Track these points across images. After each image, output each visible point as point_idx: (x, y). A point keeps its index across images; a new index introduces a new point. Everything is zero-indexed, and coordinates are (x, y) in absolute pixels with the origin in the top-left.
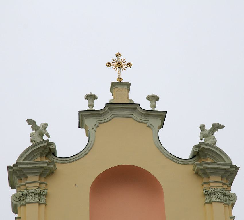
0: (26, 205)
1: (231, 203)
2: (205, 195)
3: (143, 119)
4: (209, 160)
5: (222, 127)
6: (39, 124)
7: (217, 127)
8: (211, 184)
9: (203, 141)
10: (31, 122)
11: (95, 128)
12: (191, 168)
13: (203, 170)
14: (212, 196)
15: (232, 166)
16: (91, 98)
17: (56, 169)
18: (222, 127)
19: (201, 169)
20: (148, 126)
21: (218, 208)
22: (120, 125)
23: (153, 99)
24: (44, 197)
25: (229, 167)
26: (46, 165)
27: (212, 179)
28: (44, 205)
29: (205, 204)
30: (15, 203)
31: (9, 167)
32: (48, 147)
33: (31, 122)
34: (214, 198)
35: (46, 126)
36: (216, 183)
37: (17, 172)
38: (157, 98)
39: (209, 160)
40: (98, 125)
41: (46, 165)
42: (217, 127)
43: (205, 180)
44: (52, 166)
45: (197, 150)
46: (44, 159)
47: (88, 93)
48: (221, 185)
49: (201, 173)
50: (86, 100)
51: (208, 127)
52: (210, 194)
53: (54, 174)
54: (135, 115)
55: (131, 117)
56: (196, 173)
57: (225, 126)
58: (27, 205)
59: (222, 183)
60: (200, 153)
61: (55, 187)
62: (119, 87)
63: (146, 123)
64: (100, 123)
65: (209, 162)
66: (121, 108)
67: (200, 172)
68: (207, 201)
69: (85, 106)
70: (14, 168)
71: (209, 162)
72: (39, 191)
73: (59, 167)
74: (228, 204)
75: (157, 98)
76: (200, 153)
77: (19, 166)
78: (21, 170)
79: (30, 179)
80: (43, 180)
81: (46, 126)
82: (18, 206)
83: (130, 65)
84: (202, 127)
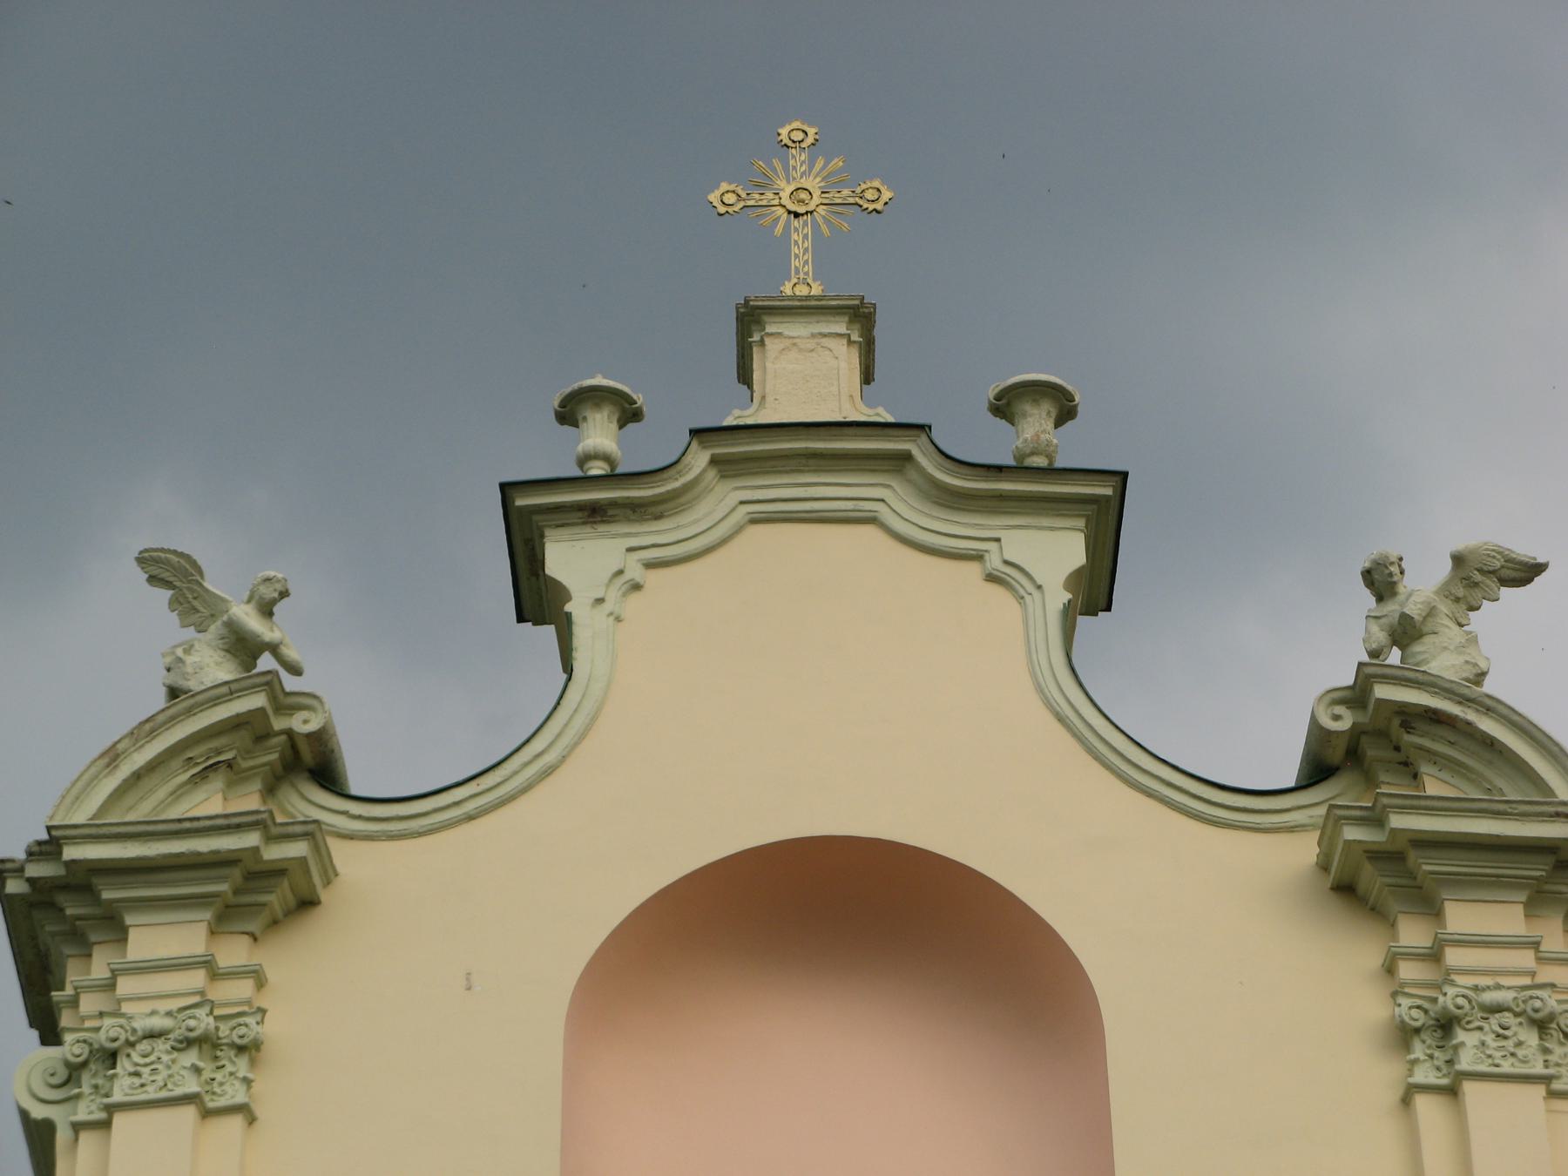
0: (106, 1125)
2: (1405, 1035)
8: (1453, 956)
11: (613, 595)
12: (1303, 851)
13: (1392, 856)
14: (1461, 1036)
17: (330, 873)
18: (1525, 573)
19: (1375, 855)
20: (992, 578)
24: (242, 1066)
26: (251, 839)
27: (1461, 917)
28: (237, 1121)
29: (1406, 1101)
30: (38, 1112)
32: (278, 724)
34: (1470, 1047)
37: (61, 899)
40: (635, 572)
41: (251, 839)
43: (1413, 933)
44: (297, 849)
45: (1345, 725)
46: (249, 801)
48: (1526, 959)
49: (1373, 883)
50: (566, 427)
52: (1446, 1025)
53: (318, 910)
55: (872, 520)
56: (1346, 889)
58: (119, 1120)
59: (1535, 945)
63: (978, 557)
64: (650, 565)
65: (1438, 804)
67: (1372, 879)
68: (1425, 1075)
69: (545, 453)
70: (33, 871)
71: (1438, 804)
72: (203, 1022)
73: (358, 866)
76: (1372, 751)
77: (71, 853)
78: (84, 879)
79: (150, 938)
80: (234, 952)
82: (62, 1136)
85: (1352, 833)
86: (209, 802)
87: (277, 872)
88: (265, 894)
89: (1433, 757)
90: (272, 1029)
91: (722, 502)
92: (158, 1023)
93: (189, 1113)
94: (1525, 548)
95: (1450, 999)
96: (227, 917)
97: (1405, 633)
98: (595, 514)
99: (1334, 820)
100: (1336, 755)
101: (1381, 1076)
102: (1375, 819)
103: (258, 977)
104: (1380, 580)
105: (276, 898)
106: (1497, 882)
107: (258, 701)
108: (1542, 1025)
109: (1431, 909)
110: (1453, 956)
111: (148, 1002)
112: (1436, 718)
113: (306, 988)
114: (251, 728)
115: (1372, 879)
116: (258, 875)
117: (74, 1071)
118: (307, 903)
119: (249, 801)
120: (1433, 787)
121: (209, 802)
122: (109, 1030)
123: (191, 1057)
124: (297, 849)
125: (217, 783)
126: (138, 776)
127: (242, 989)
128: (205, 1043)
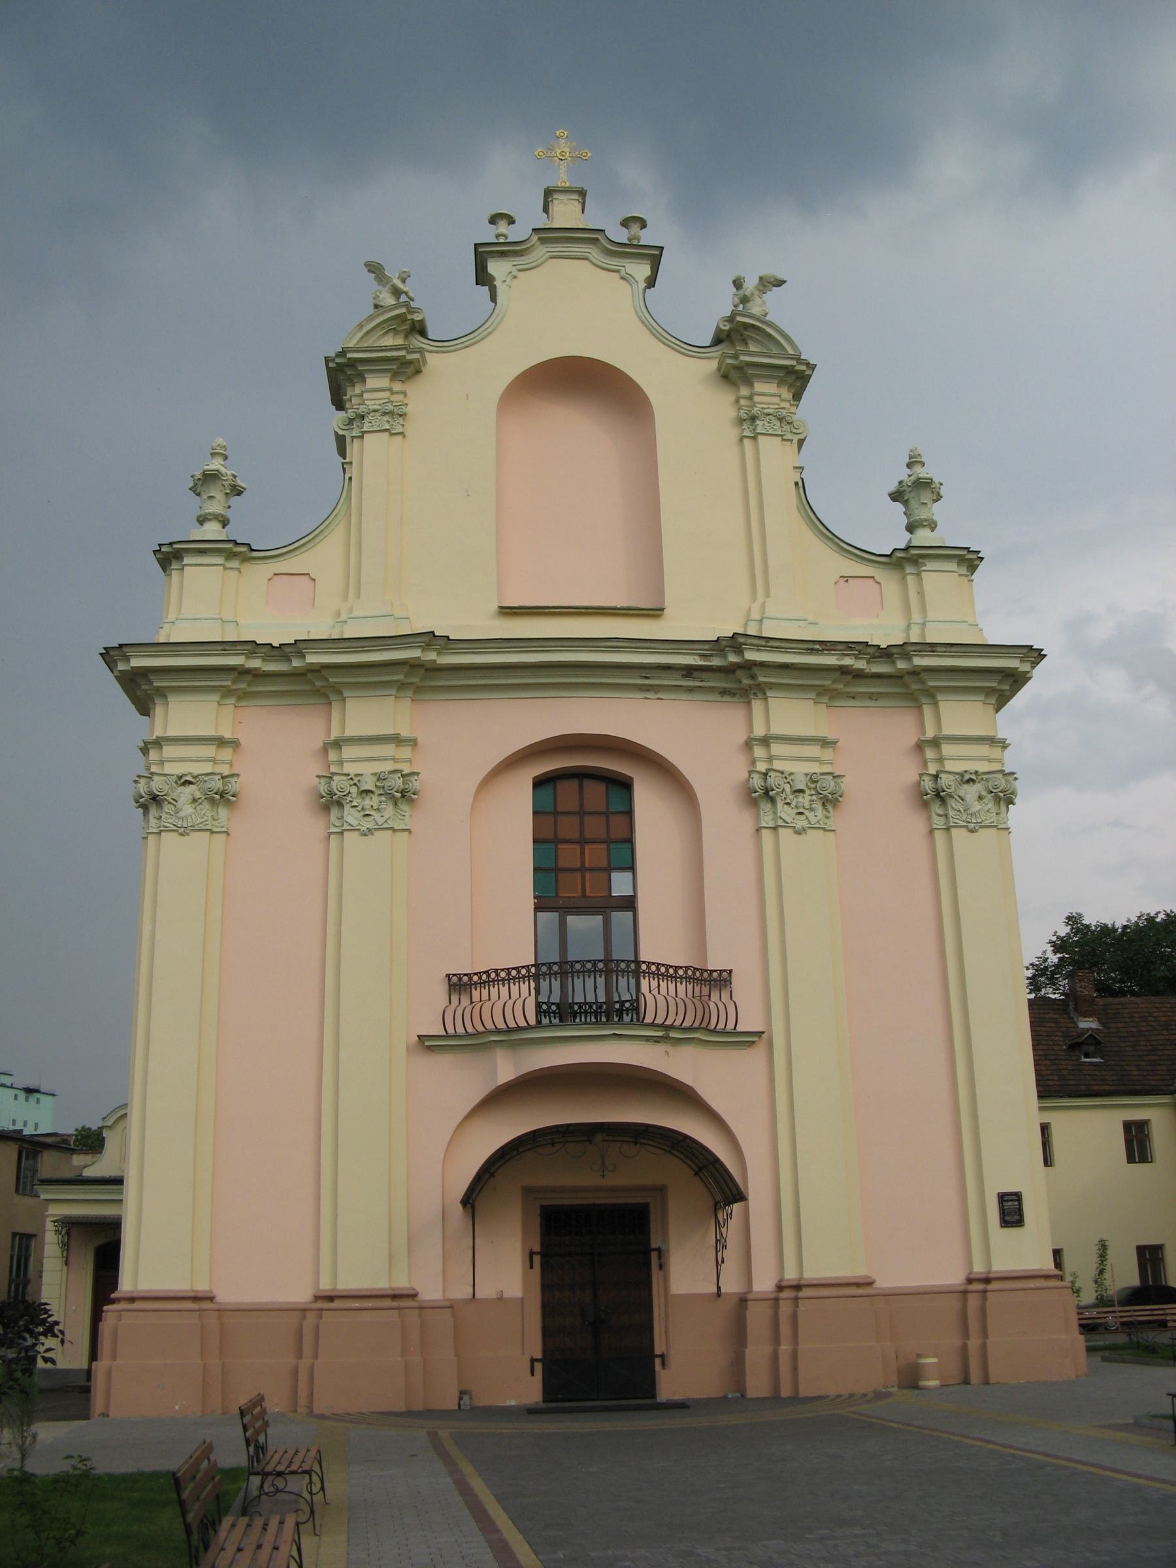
0: (362, 437)
1: (796, 438)
2: (741, 421)
8: (756, 399)
10: (375, 269)
11: (508, 280)
12: (713, 365)
15: (799, 360)
17: (425, 362)
18: (780, 283)
19: (735, 368)
20: (622, 278)
25: (793, 363)
26: (403, 353)
27: (759, 387)
28: (400, 437)
30: (341, 432)
31: (327, 360)
32: (409, 317)
33: (375, 269)
36: (769, 394)
37: (346, 369)
39: (752, 348)
40: (515, 273)
41: (403, 353)
43: (744, 391)
44: (416, 356)
45: (727, 328)
46: (400, 341)
48: (777, 400)
49: (733, 376)
52: (753, 419)
53: (421, 375)
57: (784, 282)
58: (366, 436)
62: (562, 197)
63: (618, 271)
64: (520, 270)
65: (753, 353)
68: (746, 433)
69: (488, 234)
70: (338, 360)
71: (753, 353)
72: (390, 407)
73: (435, 362)
74: (791, 441)
76: (734, 336)
77: (349, 355)
78: (353, 363)
79: (372, 382)
80: (397, 386)
82: (348, 440)
85: (729, 361)
86: (389, 341)
87: (410, 362)
88: (406, 369)
89: (752, 339)
90: (408, 410)
91: (541, 251)
92: (376, 407)
93: (386, 434)
94: (781, 276)
95: (755, 411)
96: (395, 376)
97: (745, 300)
98: (503, 254)
99: (723, 357)
100: (723, 336)
101: (733, 433)
102: (735, 357)
103: (405, 394)
104: (738, 284)
106: (770, 377)
107: (403, 310)
109: (750, 384)
110: (756, 399)
111: (373, 401)
112: (753, 326)
113: (419, 397)
114: (401, 318)
115: (734, 375)
116: (404, 363)
117: (351, 421)
118: (418, 372)
119: (400, 341)
120: (752, 348)
121: (389, 341)
122: (362, 409)
123: (386, 418)
124: (416, 356)
125: (391, 335)
126: (368, 332)
127: (401, 397)
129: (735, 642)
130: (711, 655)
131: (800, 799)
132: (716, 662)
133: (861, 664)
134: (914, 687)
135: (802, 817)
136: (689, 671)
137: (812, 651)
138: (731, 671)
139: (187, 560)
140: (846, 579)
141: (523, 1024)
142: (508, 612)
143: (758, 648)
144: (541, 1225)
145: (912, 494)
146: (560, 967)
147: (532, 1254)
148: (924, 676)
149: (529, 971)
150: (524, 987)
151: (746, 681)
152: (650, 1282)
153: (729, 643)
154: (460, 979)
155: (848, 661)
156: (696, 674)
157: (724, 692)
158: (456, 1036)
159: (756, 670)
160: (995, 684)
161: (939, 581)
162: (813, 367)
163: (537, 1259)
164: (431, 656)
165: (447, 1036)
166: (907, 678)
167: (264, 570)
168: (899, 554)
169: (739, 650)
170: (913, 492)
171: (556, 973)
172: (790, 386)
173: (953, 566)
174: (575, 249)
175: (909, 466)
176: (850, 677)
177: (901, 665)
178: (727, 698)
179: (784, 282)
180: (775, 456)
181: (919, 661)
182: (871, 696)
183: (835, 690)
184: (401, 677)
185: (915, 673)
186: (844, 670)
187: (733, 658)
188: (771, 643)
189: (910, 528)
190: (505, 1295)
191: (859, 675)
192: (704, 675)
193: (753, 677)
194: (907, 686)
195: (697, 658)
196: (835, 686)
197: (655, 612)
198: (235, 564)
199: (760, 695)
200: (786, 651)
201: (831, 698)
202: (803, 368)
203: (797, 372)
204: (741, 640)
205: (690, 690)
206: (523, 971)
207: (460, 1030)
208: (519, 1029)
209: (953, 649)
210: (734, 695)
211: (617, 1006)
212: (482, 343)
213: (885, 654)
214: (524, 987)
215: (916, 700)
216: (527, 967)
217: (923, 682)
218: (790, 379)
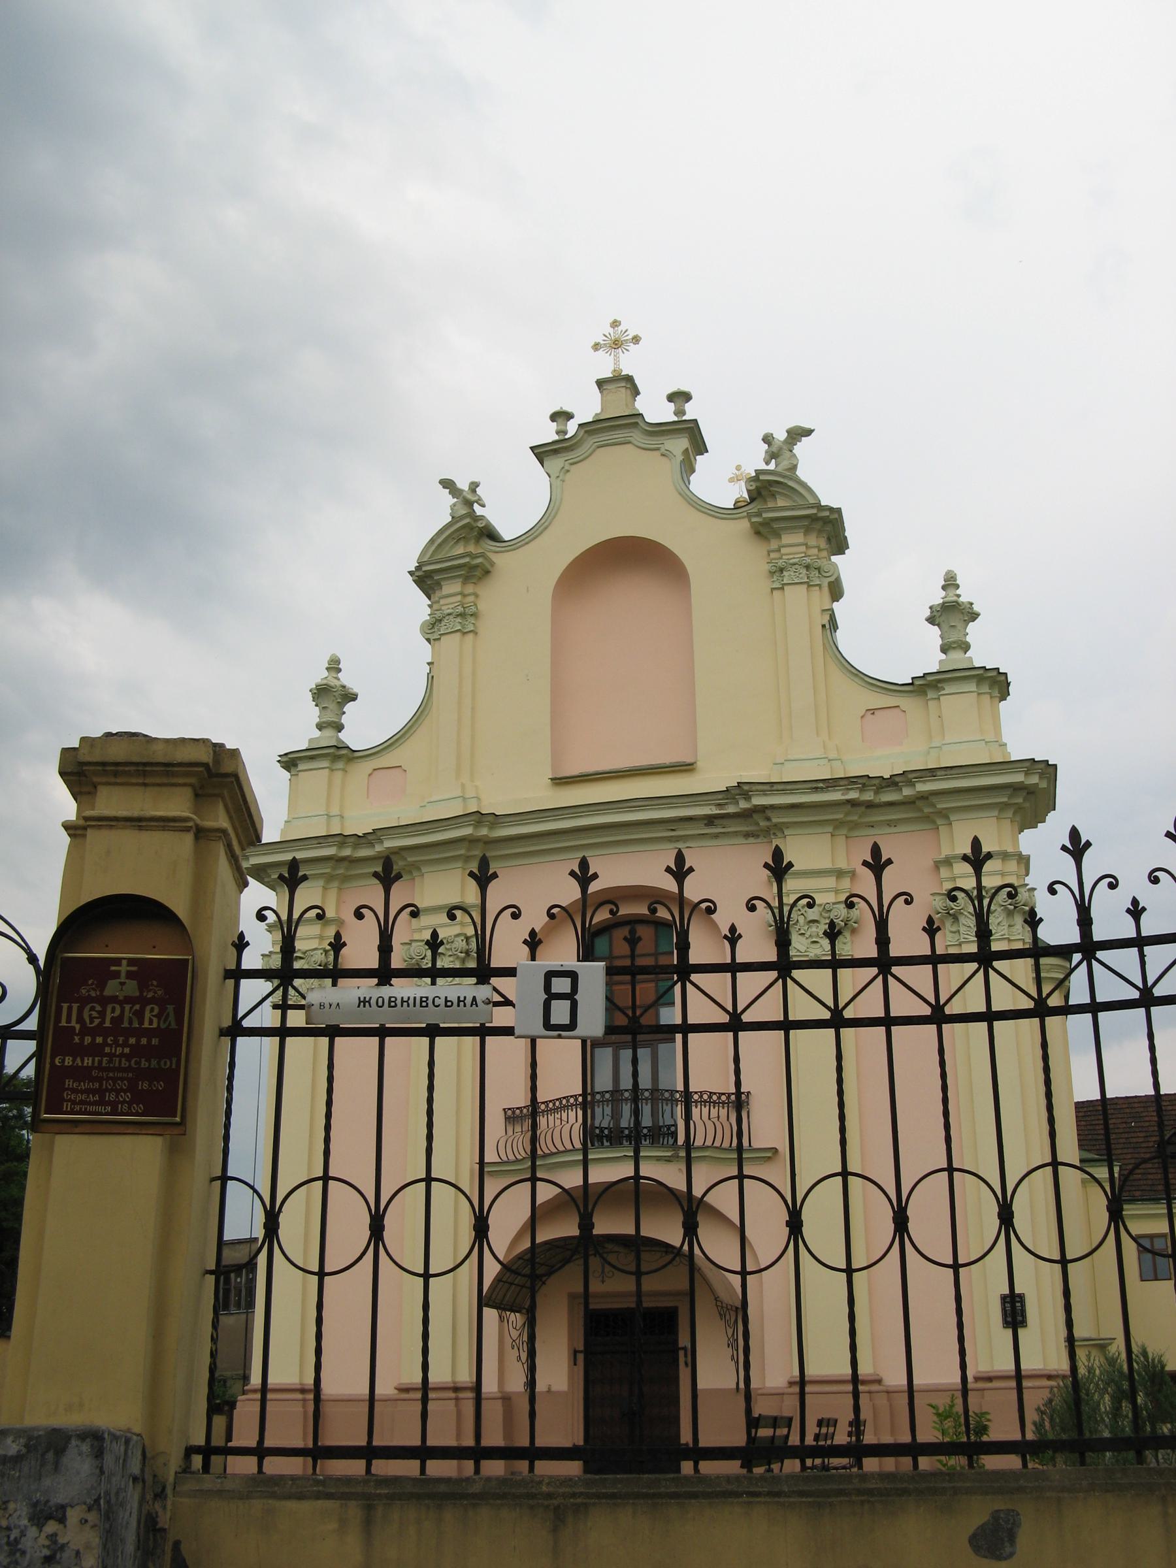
1: (825, 582)
2: (772, 573)
3: (652, 442)
4: (781, 502)
5: (808, 432)
6: (463, 485)
7: (798, 434)
9: (772, 466)
10: (447, 484)
12: (745, 525)
13: (767, 523)
14: (785, 573)
15: (819, 507)
16: (562, 416)
17: (492, 564)
18: (808, 432)
19: (761, 524)
20: (663, 455)
21: (796, 596)
22: (619, 462)
23: (680, 397)
24: (472, 620)
25: (814, 511)
26: (467, 560)
27: (787, 539)
28: (471, 636)
33: (447, 484)
34: (787, 576)
35: (474, 486)
36: (794, 544)
38: (686, 397)
41: (467, 560)
42: (798, 434)
43: (774, 544)
46: (471, 548)
47: (557, 409)
48: (803, 548)
49: (765, 530)
51: (781, 436)
52: (781, 570)
54: (636, 436)
55: (629, 442)
56: (758, 533)
57: (812, 431)
60: (763, 488)
61: (492, 599)
63: (658, 449)
66: (618, 425)
72: (460, 609)
73: (502, 560)
75: (686, 397)
76: (764, 493)
80: (470, 589)
81: (474, 486)
83: (636, 340)
84: (768, 439)
85: (754, 520)
86: (460, 550)
88: (476, 573)
89: (779, 493)
90: (482, 606)
91: (591, 441)
93: (458, 634)
94: (807, 425)
95: (780, 563)
96: (466, 579)
100: (755, 495)
101: (765, 584)
102: (759, 514)
103: (476, 595)
105: (478, 573)
106: (795, 527)
107: (467, 520)
108: (807, 567)
109: (779, 536)
115: (761, 529)
118: (487, 572)
120: (781, 502)
121: (460, 550)
123: (459, 620)
125: (462, 543)
126: (440, 545)
128: (462, 615)
129: (742, 790)
130: (726, 804)
131: (814, 929)
132: (731, 809)
133: (868, 796)
134: (926, 810)
135: (818, 946)
136: (710, 820)
137: (816, 790)
138: (746, 814)
139: (301, 767)
140: (873, 711)
141: (569, 1147)
142: (560, 781)
143: (764, 793)
144: (585, 1325)
145: (943, 618)
146: (612, 1095)
147: (575, 1352)
148: (934, 799)
149: (576, 1100)
150: (572, 1114)
151: (763, 824)
152: (678, 1377)
153: (738, 791)
154: (514, 1113)
155: (853, 795)
156: (717, 822)
157: (747, 835)
158: (508, 1162)
159: (769, 813)
160: (1005, 799)
161: (959, 704)
162: (839, 511)
163: (581, 1357)
164: (484, 831)
165: (503, 1163)
166: (918, 803)
167: (367, 766)
168: (917, 682)
169: (747, 796)
170: (952, 614)
171: (608, 1101)
172: (820, 531)
173: (972, 686)
174: (618, 435)
175: (944, 588)
176: (863, 809)
177: (907, 792)
178: (751, 840)
179: (812, 431)
180: (800, 603)
181: (922, 787)
182: (889, 823)
183: (851, 821)
184: (462, 852)
185: (925, 797)
186: (853, 803)
187: (743, 805)
188: (775, 787)
189: (944, 649)
190: (554, 1389)
191: (870, 805)
192: (724, 822)
193: (768, 819)
194: (921, 810)
195: (713, 808)
196: (849, 818)
197: (685, 768)
198: (340, 765)
199: (779, 835)
200: (792, 792)
201: (851, 829)
202: (827, 513)
203: (822, 518)
204: (746, 788)
205: (716, 836)
206: (572, 1100)
207: (512, 1157)
208: (553, 1154)
209: (953, 771)
210: (758, 836)
211: (627, 1132)
212: (540, 538)
213: (892, 782)
214: (572, 1114)
215: (934, 822)
216: (575, 1097)
217: (934, 806)
218: (818, 525)
